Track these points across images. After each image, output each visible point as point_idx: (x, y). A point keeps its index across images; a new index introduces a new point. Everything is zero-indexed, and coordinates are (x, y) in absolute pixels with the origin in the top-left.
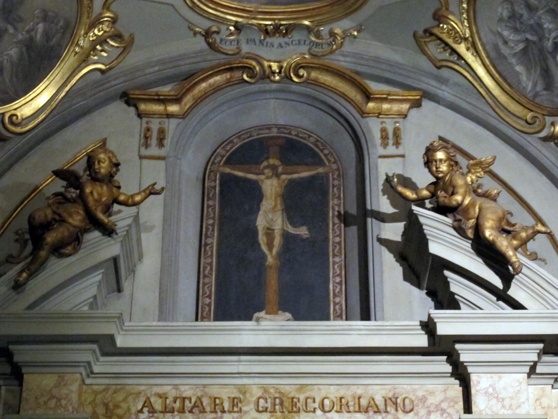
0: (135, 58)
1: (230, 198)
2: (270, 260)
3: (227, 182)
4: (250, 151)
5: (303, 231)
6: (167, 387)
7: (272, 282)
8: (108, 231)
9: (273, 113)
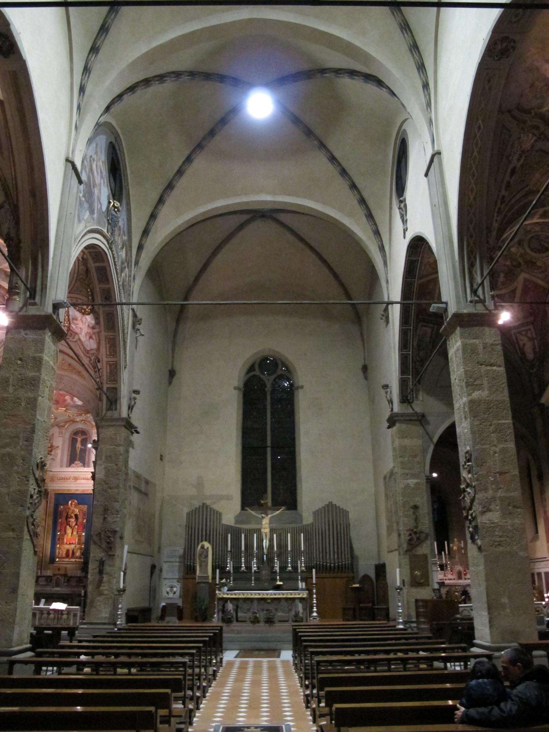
0: (58, 420)
1: (73, 441)
2: (78, 452)
3: (73, 439)
4: (76, 433)
5: (83, 448)
6: (60, 476)
7: (78, 457)
8: (51, 455)
9: (80, 426)
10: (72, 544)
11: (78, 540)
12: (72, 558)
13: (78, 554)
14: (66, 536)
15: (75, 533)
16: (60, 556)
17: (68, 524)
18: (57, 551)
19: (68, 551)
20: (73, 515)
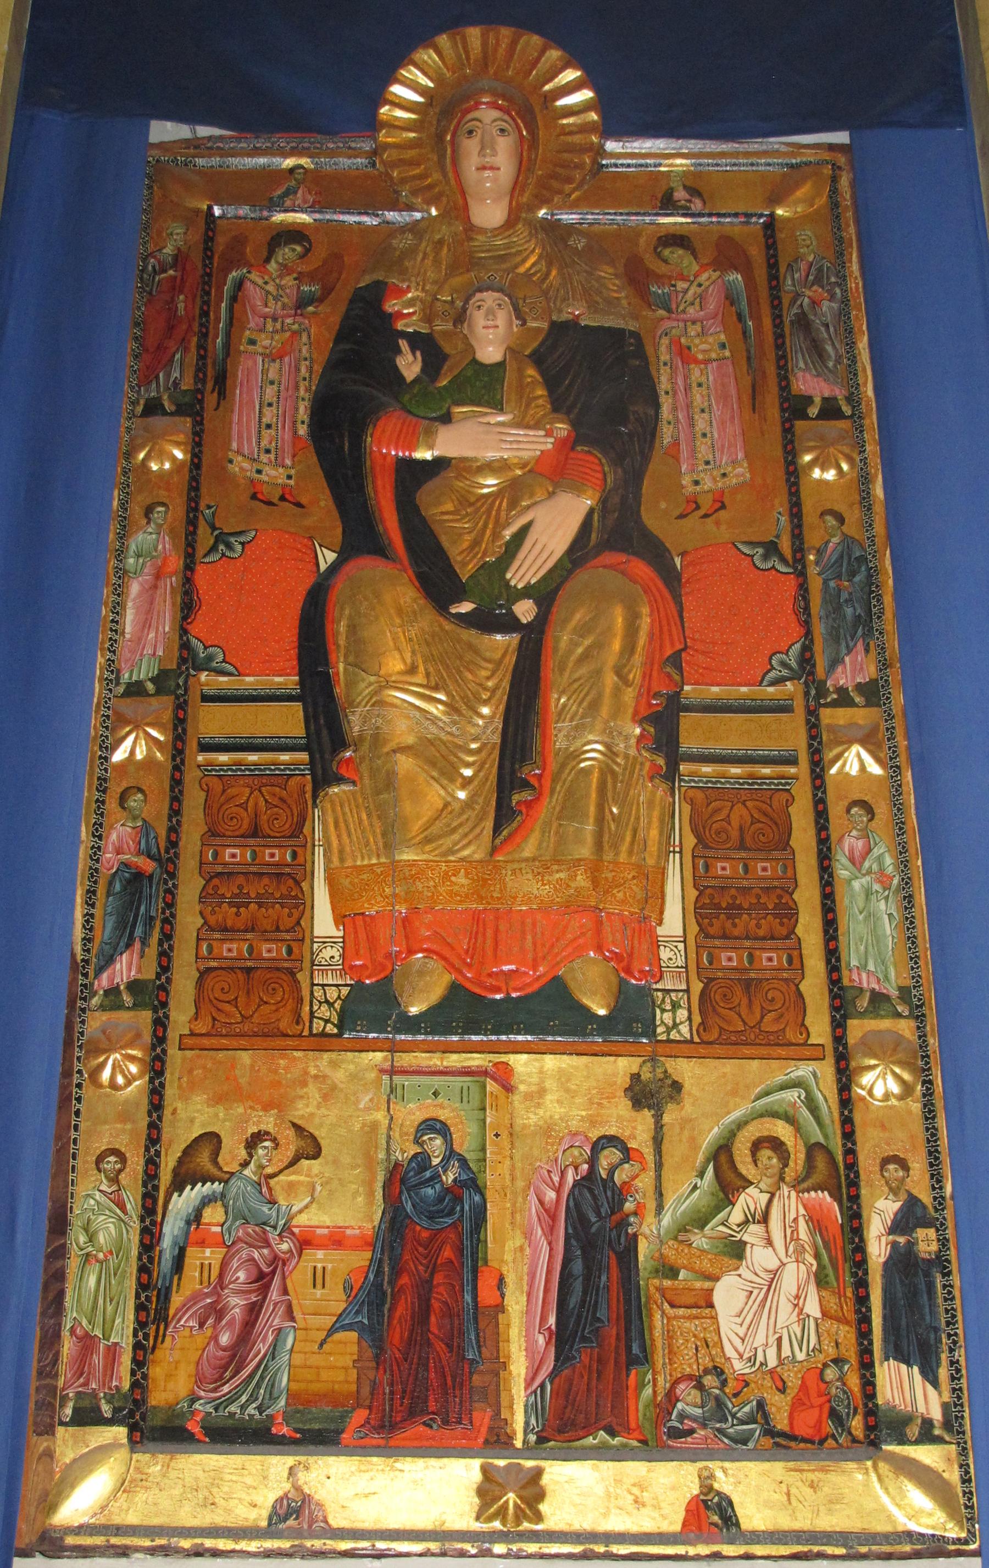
10: (552, 1015)
11: (714, 911)
12: (585, 1412)
13: (762, 1306)
14: (335, 835)
15: (591, 738)
16: (172, 1383)
17: (387, 518)
18: (102, 1221)
19: (430, 1220)
20: (491, 335)
